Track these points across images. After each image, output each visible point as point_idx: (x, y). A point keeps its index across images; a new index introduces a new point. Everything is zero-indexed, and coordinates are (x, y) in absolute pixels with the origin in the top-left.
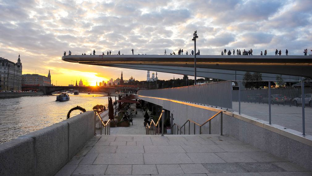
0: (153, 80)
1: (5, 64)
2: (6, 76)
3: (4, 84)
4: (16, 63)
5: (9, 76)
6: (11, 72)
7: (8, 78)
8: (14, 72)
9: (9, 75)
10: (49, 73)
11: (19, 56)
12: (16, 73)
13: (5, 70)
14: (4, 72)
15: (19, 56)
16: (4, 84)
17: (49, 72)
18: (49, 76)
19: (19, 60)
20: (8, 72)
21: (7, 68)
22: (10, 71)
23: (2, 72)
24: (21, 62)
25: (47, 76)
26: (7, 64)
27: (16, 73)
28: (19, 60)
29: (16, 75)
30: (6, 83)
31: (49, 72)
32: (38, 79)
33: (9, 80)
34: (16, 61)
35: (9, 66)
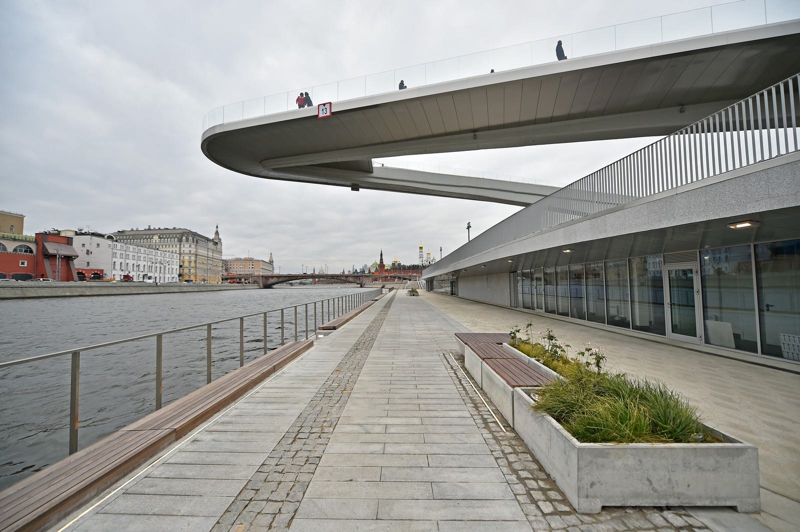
0: (428, 263)
1: (191, 238)
2: (193, 258)
3: (189, 271)
5: (197, 259)
6: (202, 251)
7: (195, 262)
8: (206, 253)
9: (198, 256)
11: (217, 227)
12: (210, 254)
13: (190, 249)
14: (188, 252)
15: (217, 227)
16: (189, 271)
19: (217, 233)
20: (196, 251)
21: (193, 246)
22: (198, 250)
23: (192, 253)
24: (220, 236)
26: (193, 239)
27: (210, 254)
28: (217, 233)
29: (212, 257)
30: (193, 271)
32: (253, 265)
33: (197, 266)
34: (211, 236)
35: (197, 243)
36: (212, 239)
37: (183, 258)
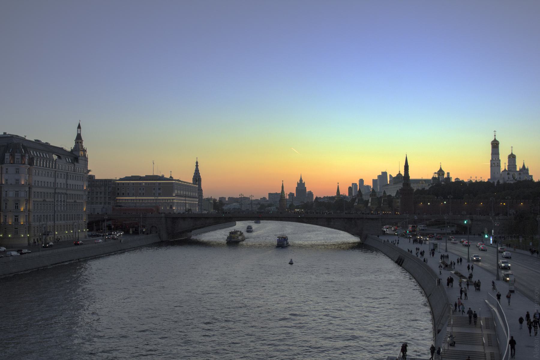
4: (72, 150)
8: (52, 180)
9: (33, 190)
10: (197, 171)
11: (79, 127)
12: (61, 181)
15: (79, 127)
17: (197, 166)
18: (197, 178)
19: (79, 138)
24: (85, 145)
25: (189, 179)
27: (61, 181)
28: (79, 138)
31: (197, 166)
34: (69, 145)
35: (31, 163)
36: (69, 150)
37: (6, 195)
